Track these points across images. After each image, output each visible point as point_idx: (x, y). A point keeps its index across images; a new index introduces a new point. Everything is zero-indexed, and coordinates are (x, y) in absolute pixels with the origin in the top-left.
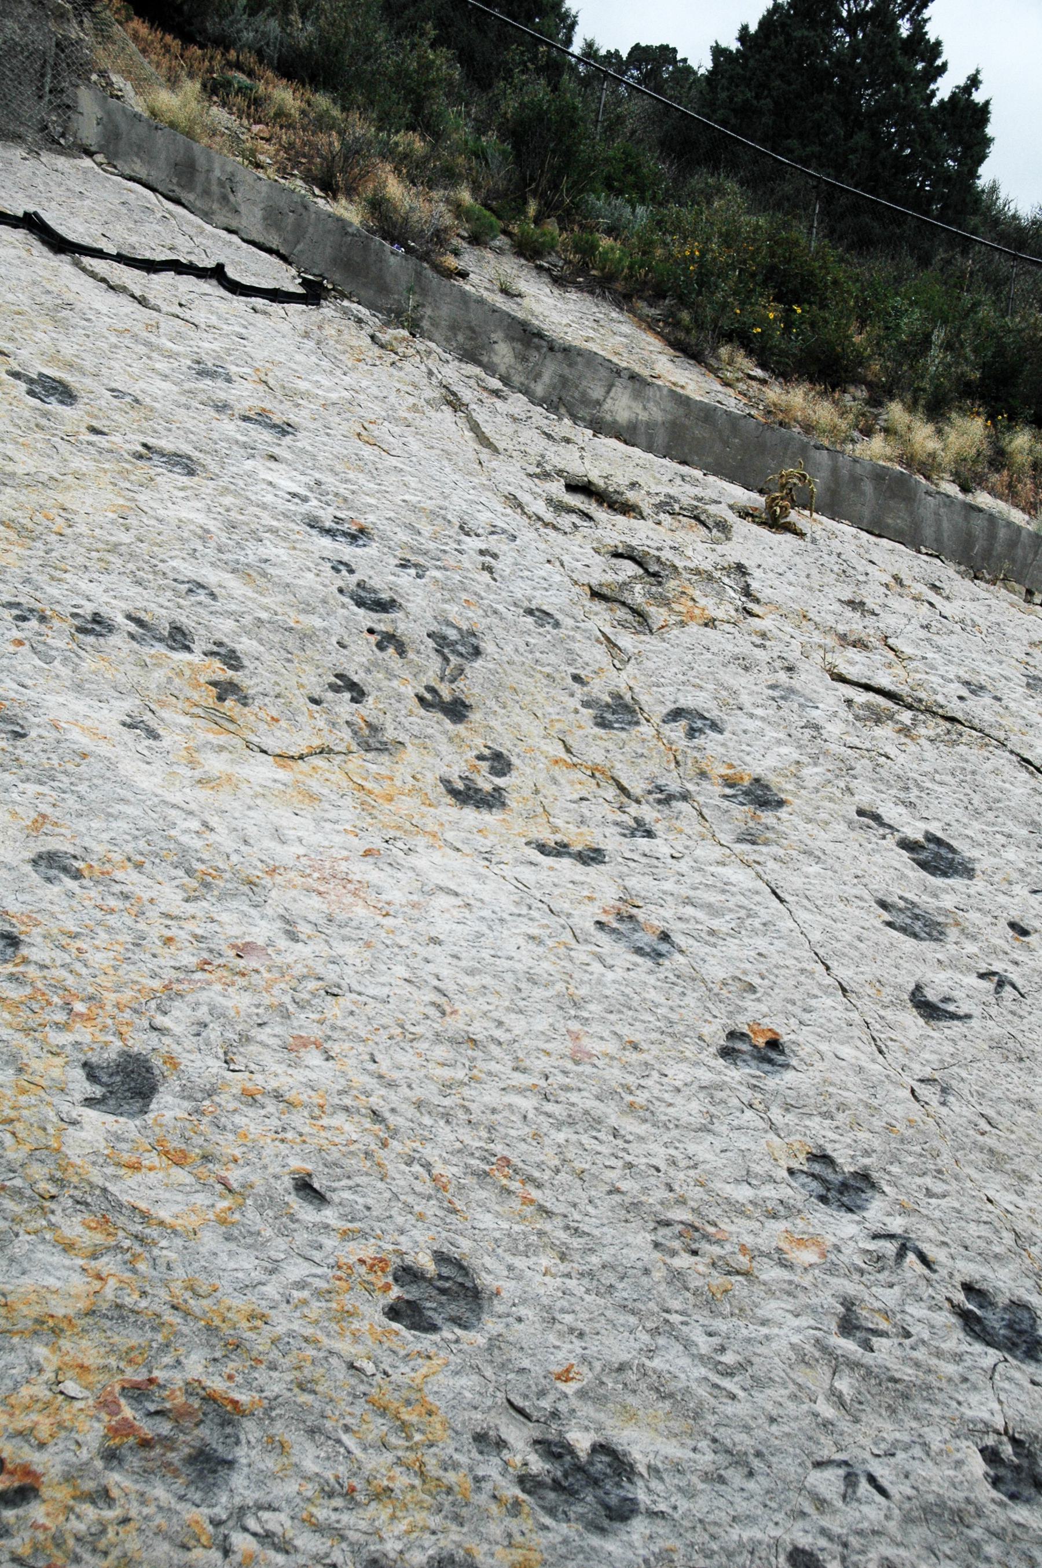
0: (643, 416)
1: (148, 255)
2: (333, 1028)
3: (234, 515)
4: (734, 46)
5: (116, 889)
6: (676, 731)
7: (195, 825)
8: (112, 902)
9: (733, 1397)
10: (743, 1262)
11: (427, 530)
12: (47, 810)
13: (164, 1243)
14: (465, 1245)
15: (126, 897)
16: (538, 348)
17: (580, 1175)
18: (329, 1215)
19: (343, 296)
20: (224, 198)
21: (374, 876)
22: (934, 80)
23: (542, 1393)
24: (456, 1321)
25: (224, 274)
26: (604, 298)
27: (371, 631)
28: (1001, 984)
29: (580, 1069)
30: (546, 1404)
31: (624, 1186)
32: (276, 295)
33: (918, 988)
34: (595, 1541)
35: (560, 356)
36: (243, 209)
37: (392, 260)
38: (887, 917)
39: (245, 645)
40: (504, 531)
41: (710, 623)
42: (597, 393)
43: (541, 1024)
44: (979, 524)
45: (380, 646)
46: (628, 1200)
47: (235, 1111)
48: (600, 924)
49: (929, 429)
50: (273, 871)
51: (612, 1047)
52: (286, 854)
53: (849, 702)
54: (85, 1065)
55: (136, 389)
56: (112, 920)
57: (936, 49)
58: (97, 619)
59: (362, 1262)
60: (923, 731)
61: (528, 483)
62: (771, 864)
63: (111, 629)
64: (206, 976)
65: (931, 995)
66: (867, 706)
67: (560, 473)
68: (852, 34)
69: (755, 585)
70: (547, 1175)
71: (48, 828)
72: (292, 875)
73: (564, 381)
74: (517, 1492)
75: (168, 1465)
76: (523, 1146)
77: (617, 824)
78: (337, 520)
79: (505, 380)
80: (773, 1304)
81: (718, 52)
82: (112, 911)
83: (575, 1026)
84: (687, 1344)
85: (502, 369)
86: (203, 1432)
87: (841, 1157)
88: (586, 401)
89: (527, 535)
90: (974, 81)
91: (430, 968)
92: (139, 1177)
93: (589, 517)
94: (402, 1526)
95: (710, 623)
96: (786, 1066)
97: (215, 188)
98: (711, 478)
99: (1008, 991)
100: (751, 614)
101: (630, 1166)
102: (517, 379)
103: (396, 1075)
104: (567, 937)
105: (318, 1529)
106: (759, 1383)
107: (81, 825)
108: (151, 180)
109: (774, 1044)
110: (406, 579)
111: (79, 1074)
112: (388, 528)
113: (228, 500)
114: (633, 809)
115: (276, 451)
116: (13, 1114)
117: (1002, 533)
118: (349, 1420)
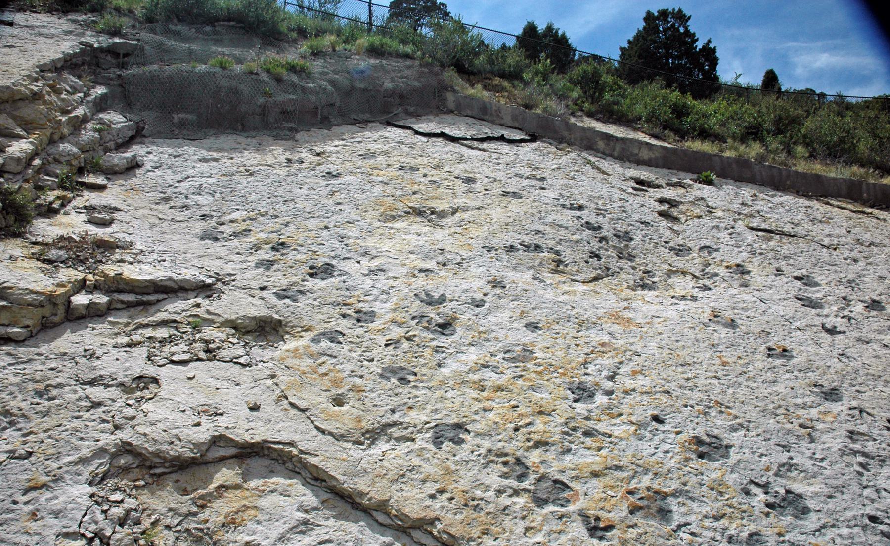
0: (653, 156)
1: (480, 137)
2: (643, 366)
3: (540, 208)
4: (626, 46)
5: (554, 331)
6: (705, 253)
7: (569, 307)
8: (555, 336)
9: (826, 469)
10: (809, 424)
11: (600, 203)
12: (522, 309)
13: (620, 443)
14: (716, 432)
15: (558, 333)
16: (612, 140)
17: (742, 403)
18: (667, 427)
19: (542, 137)
20: (498, 115)
21: (630, 315)
22: (695, 43)
23: (762, 476)
24: (721, 456)
25: (505, 138)
26: (620, 124)
27: (596, 237)
28: (849, 320)
29: (726, 368)
30: (764, 479)
31: (760, 404)
32: (522, 141)
33: (823, 326)
34: (801, 522)
35: (621, 142)
36: (504, 117)
37: (557, 122)
38: (801, 303)
39: (559, 247)
40: (624, 199)
41: (699, 217)
42: (636, 151)
43: (708, 355)
44: (775, 172)
45: (600, 241)
46: (762, 409)
47: (624, 398)
48: (710, 320)
49: (744, 146)
50: (599, 318)
51: (734, 359)
52: (601, 312)
53: (757, 236)
54: (569, 389)
55: (493, 175)
56: (557, 341)
57: (694, 35)
58: (512, 246)
59: (686, 441)
60: (784, 241)
61: (624, 183)
62: (756, 292)
63: (518, 250)
64: (594, 355)
65: (828, 326)
66: (764, 236)
67: (632, 178)
68: (665, 35)
69: (710, 204)
70: (732, 404)
71: (525, 315)
72: (606, 319)
73: (623, 149)
74: (767, 510)
75: (651, 514)
76: (721, 396)
77: (697, 287)
78: (571, 204)
79: (603, 153)
80: (825, 436)
81: (621, 49)
82: (556, 339)
83: (718, 354)
84: (803, 453)
85: (602, 150)
86: (658, 502)
87: (826, 384)
88: (632, 154)
89: (631, 200)
90: (709, 41)
91: (663, 342)
92: (601, 423)
93: (647, 191)
94: (734, 526)
95: (699, 217)
96: (792, 357)
97: (494, 113)
98: (680, 173)
99: (853, 321)
100: (711, 213)
101: (757, 397)
102: (607, 152)
103: (670, 378)
104: (702, 326)
105: (707, 529)
106: (832, 463)
107: (535, 312)
108: (473, 115)
109: (785, 350)
110: (600, 218)
111: (569, 392)
112: (588, 204)
113: (536, 204)
114: (700, 281)
115: (543, 186)
116: (555, 408)
117: (784, 173)
118: (702, 493)
